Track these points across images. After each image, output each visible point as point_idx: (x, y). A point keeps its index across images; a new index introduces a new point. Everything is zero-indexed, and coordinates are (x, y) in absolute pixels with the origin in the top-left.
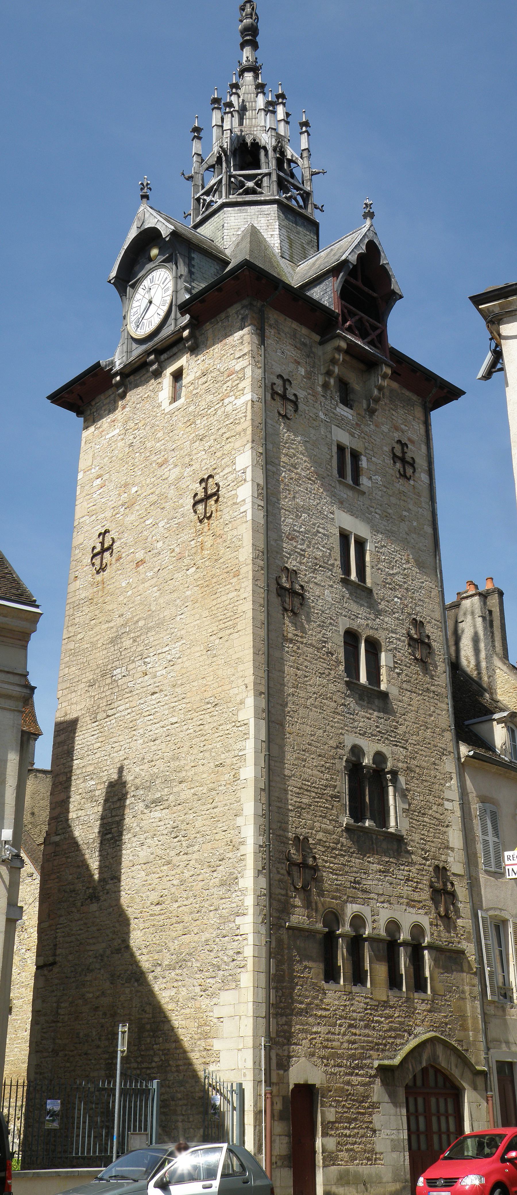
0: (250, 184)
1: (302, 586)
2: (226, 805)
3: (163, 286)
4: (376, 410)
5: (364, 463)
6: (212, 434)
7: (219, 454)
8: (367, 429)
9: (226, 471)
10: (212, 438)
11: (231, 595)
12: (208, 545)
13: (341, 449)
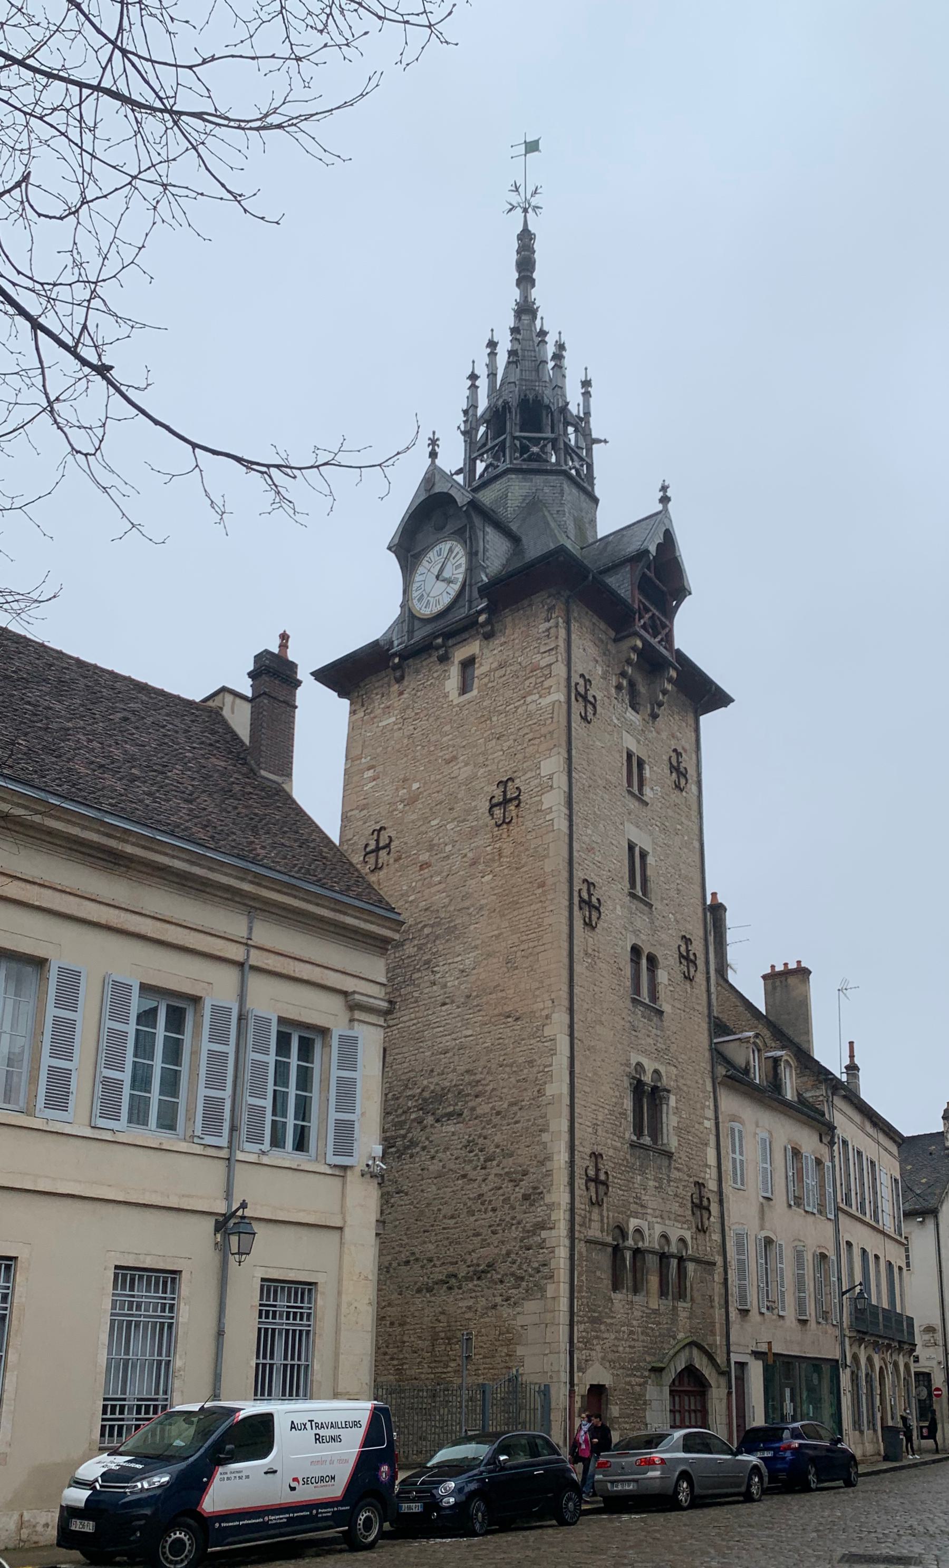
0: (535, 449)
1: (598, 900)
2: (529, 1120)
3: (454, 562)
4: (658, 716)
5: (647, 773)
6: (512, 733)
7: (520, 756)
8: (650, 736)
9: (529, 775)
10: (512, 737)
11: (533, 907)
12: (507, 852)
13: (630, 755)
